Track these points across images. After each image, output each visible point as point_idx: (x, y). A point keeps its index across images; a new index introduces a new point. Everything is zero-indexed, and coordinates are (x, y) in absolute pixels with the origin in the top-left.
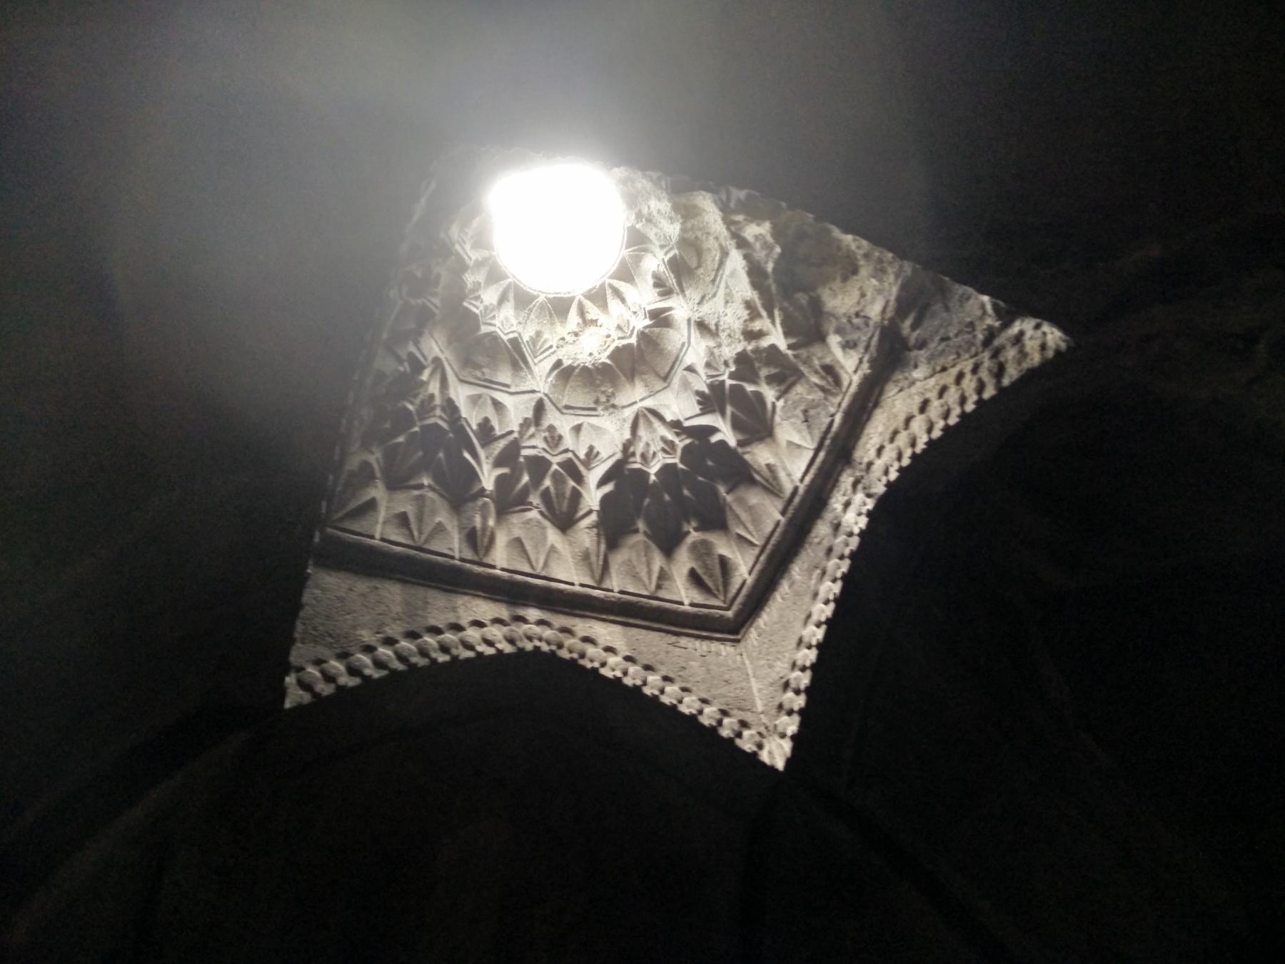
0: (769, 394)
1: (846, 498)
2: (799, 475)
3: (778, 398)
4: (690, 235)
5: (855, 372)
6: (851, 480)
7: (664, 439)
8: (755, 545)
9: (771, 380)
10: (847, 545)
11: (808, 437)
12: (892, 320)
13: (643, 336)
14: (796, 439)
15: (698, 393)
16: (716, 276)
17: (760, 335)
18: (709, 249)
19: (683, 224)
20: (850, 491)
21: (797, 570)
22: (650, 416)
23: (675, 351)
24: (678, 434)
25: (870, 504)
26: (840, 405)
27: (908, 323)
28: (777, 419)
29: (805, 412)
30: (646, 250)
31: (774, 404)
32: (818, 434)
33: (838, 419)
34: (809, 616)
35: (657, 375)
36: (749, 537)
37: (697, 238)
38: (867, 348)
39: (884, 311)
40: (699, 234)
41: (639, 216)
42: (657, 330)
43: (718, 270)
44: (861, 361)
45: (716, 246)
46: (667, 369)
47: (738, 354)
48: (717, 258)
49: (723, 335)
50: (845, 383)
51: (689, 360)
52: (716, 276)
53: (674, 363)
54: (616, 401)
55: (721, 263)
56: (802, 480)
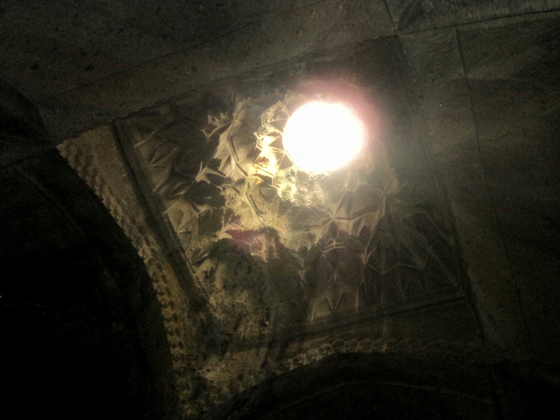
0: (203, 209)
1: (151, 243)
2: (169, 215)
3: (199, 215)
4: (273, 200)
5: (197, 277)
6: (157, 250)
7: (216, 127)
8: (150, 159)
9: (208, 212)
10: (135, 237)
11: (181, 231)
12: (208, 310)
13: (254, 140)
14: (184, 222)
15: (221, 161)
16: (252, 200)
17: (226, 221)
18: (264, 204)
19: (280, 199)
20: (154, 247)
21: (129, 187)
22: (227, 124)
23: (238, 152)
24: (212, 136)
25: (146, 261)
26: (188, 260)
27: (204, 318)
28: (192, 210)
29: (190, 232)
30: (278, 163)
31: (197, 211)
32: (180, 237)
33: (183, 255)
34: (112, 194)
35: (235, 135)
36: (154, 159)
37: (271, 202)
38: (203, 289)
39: (212, 306)
40: (271, 204)
41: (293, 173)
42: (250, 148)
43: (254, 203)
44: (200, 283)
45: (263, 211)
46: (234, 142)
47: (225, 200)
48: (258, 206)
49: (233, 192)
50: (194, 268)
51: (233, 162)
52: (252, 200)
53: (234, 148)
54: (244, 110)
55: (255, 207)
56: (166, 216)
